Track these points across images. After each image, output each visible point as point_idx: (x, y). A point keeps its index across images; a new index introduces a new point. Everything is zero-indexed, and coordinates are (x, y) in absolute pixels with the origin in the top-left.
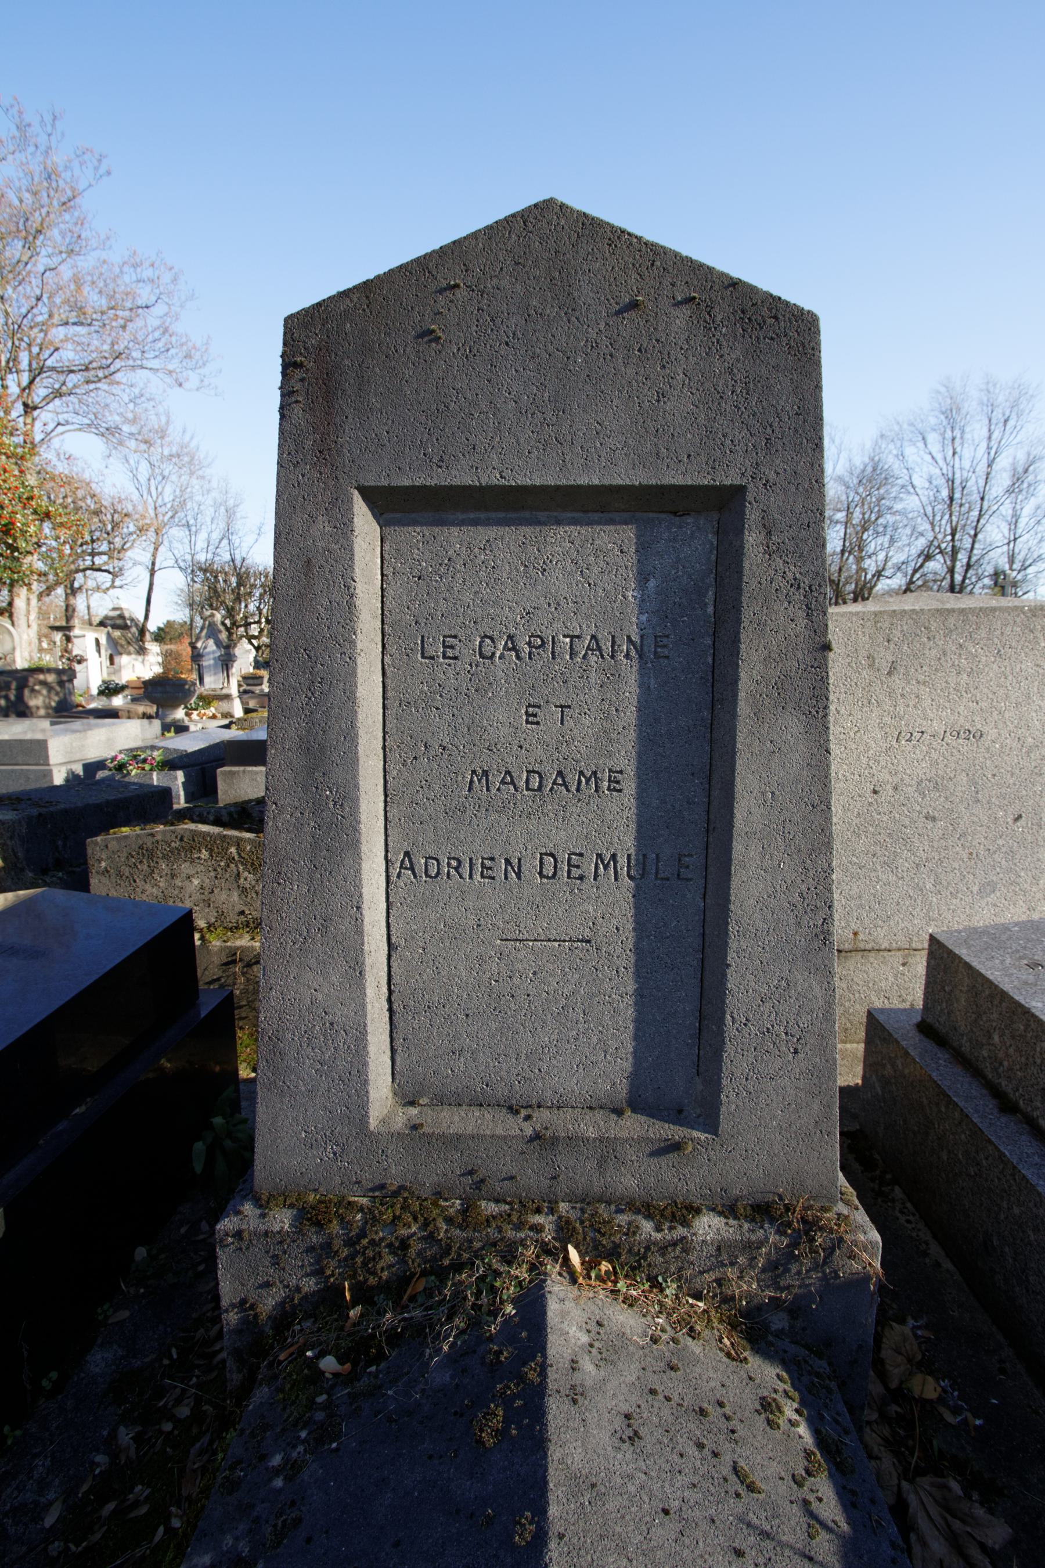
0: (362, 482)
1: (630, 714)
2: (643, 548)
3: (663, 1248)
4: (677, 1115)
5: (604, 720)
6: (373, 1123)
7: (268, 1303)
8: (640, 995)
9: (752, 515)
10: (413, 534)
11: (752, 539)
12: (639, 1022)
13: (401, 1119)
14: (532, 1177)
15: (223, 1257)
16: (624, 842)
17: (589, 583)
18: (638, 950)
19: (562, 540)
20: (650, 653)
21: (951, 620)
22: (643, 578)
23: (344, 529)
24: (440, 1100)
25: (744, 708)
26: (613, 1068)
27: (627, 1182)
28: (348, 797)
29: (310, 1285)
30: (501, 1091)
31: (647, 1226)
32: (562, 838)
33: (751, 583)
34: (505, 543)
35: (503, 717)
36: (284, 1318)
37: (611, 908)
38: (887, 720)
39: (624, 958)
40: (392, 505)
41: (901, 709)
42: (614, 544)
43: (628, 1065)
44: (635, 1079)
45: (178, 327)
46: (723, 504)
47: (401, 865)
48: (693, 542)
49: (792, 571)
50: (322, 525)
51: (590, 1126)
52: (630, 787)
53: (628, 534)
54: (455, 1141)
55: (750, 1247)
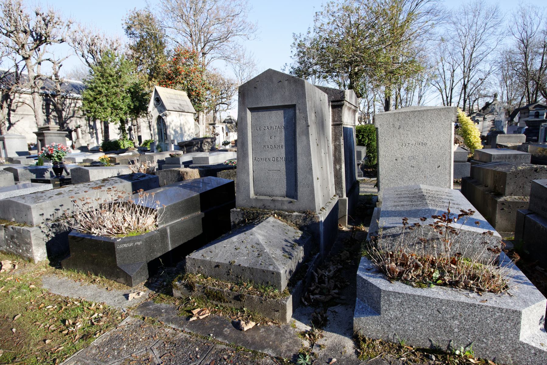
0: (249, 107)
1: (284, 136)
2: (284, 113)
3: (289, 216)
4: (293, 198)
5: (280, 138)
6: (251, 197)
7: (237, 222)
8: (287, 179)
9: (297, 108)
10: (255, 113)
11: (297, 111)
12: (287, 183)
13: (255, 197)
14: (272, 206)
15: (231, 214)
16: (283, 155)
17: (277, 119)
18: (286, 172)
19: (274, 113)
20: (286, 128)
21: (416, 114)
22: (284, 118)
23: (246, 113)
24: (260, 195)
25: (297, 135)
26: (284, 191)
27: (285, 207)
28: (247, 150)
29: (242, 219)
30: (268, 194)
31: (287, 213)
32: (275, 155)
33: (297, 117)
34: (267, 113)
35: (267, 138)
36: (239, 223)
37: (282, 166)
38: (399, 141)
39: (284, 173)
40: (252, 110)
41: (402, 138)
42: (281, 113)
43: (286, 190)
44: (287, 192)
45: (248, 20)
46: (294, 106)
47: (255, 159)
48: (291, 111)
49: (303, 115)
50: (243, 113)
51: (280, 199)
52: (284, 147)
53: (282, 111)
54: (262, 200)
55: (300, 216)
